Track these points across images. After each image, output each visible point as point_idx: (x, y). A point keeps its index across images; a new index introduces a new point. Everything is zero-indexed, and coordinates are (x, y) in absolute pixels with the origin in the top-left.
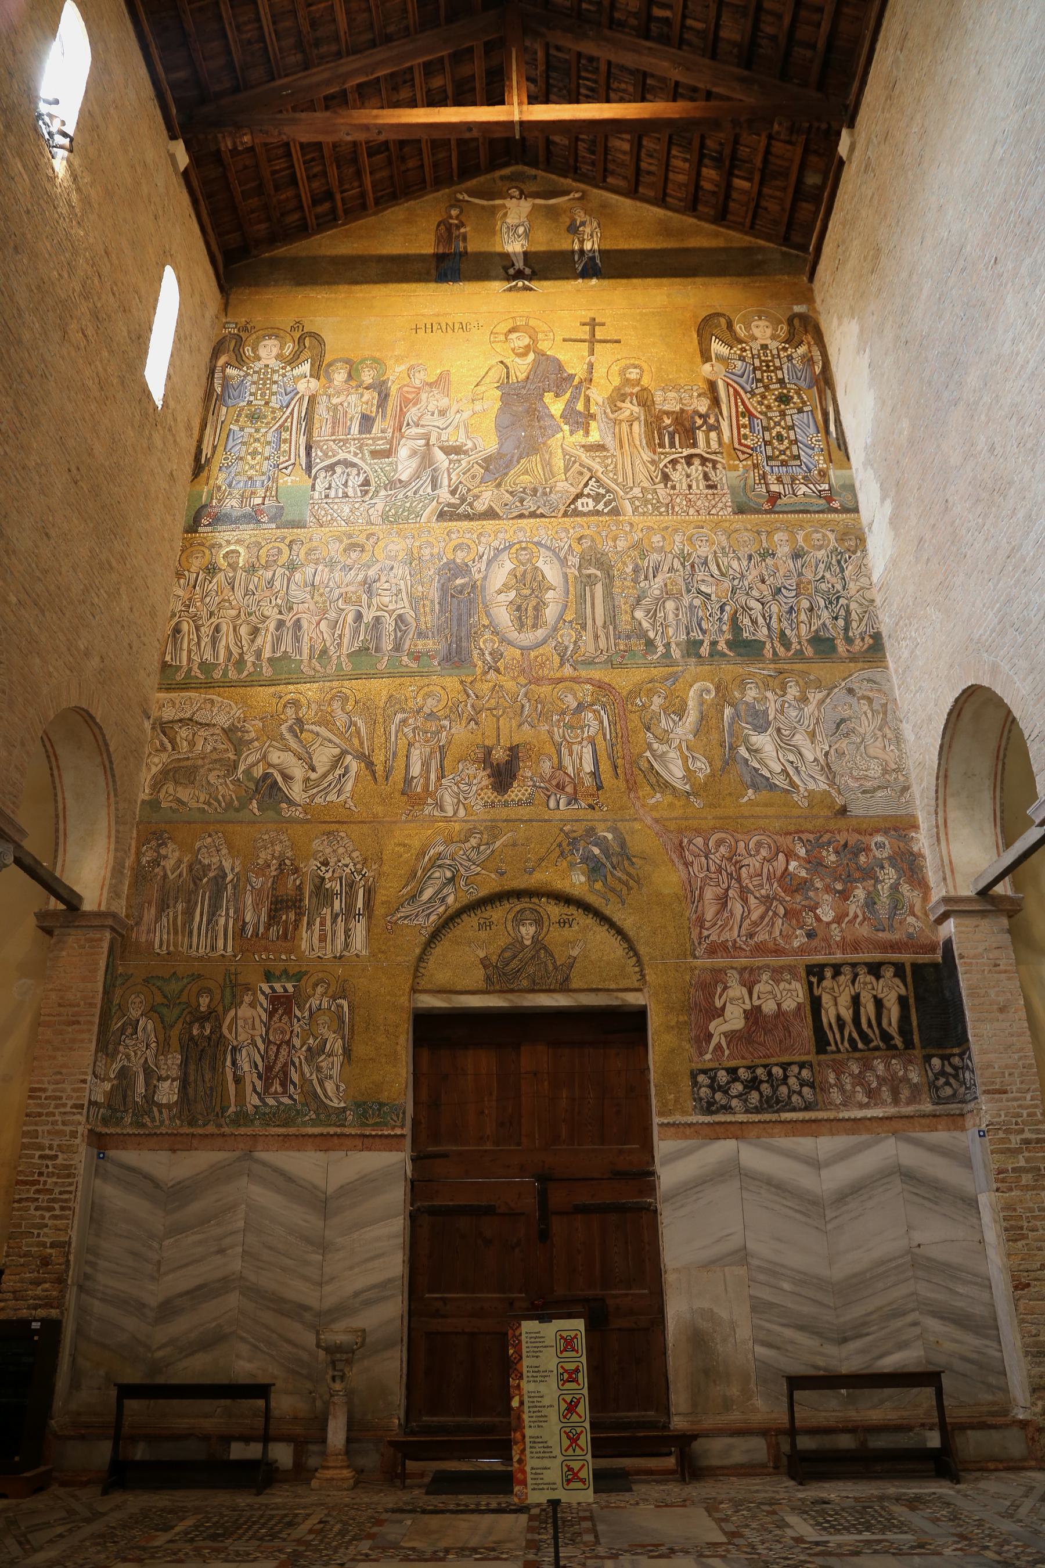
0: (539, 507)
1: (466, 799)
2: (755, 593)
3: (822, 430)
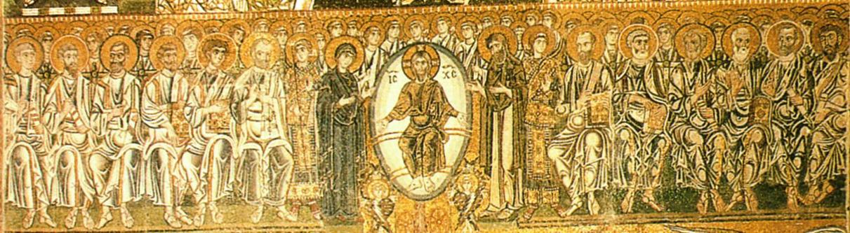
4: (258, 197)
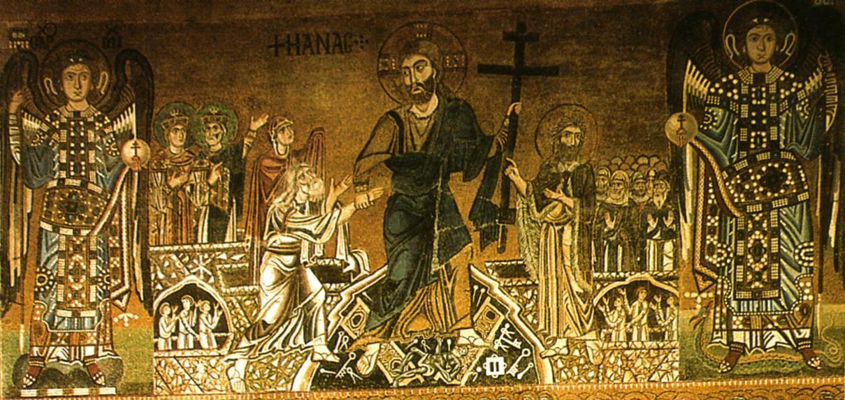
0: (437, 370)
3: (817, 237)
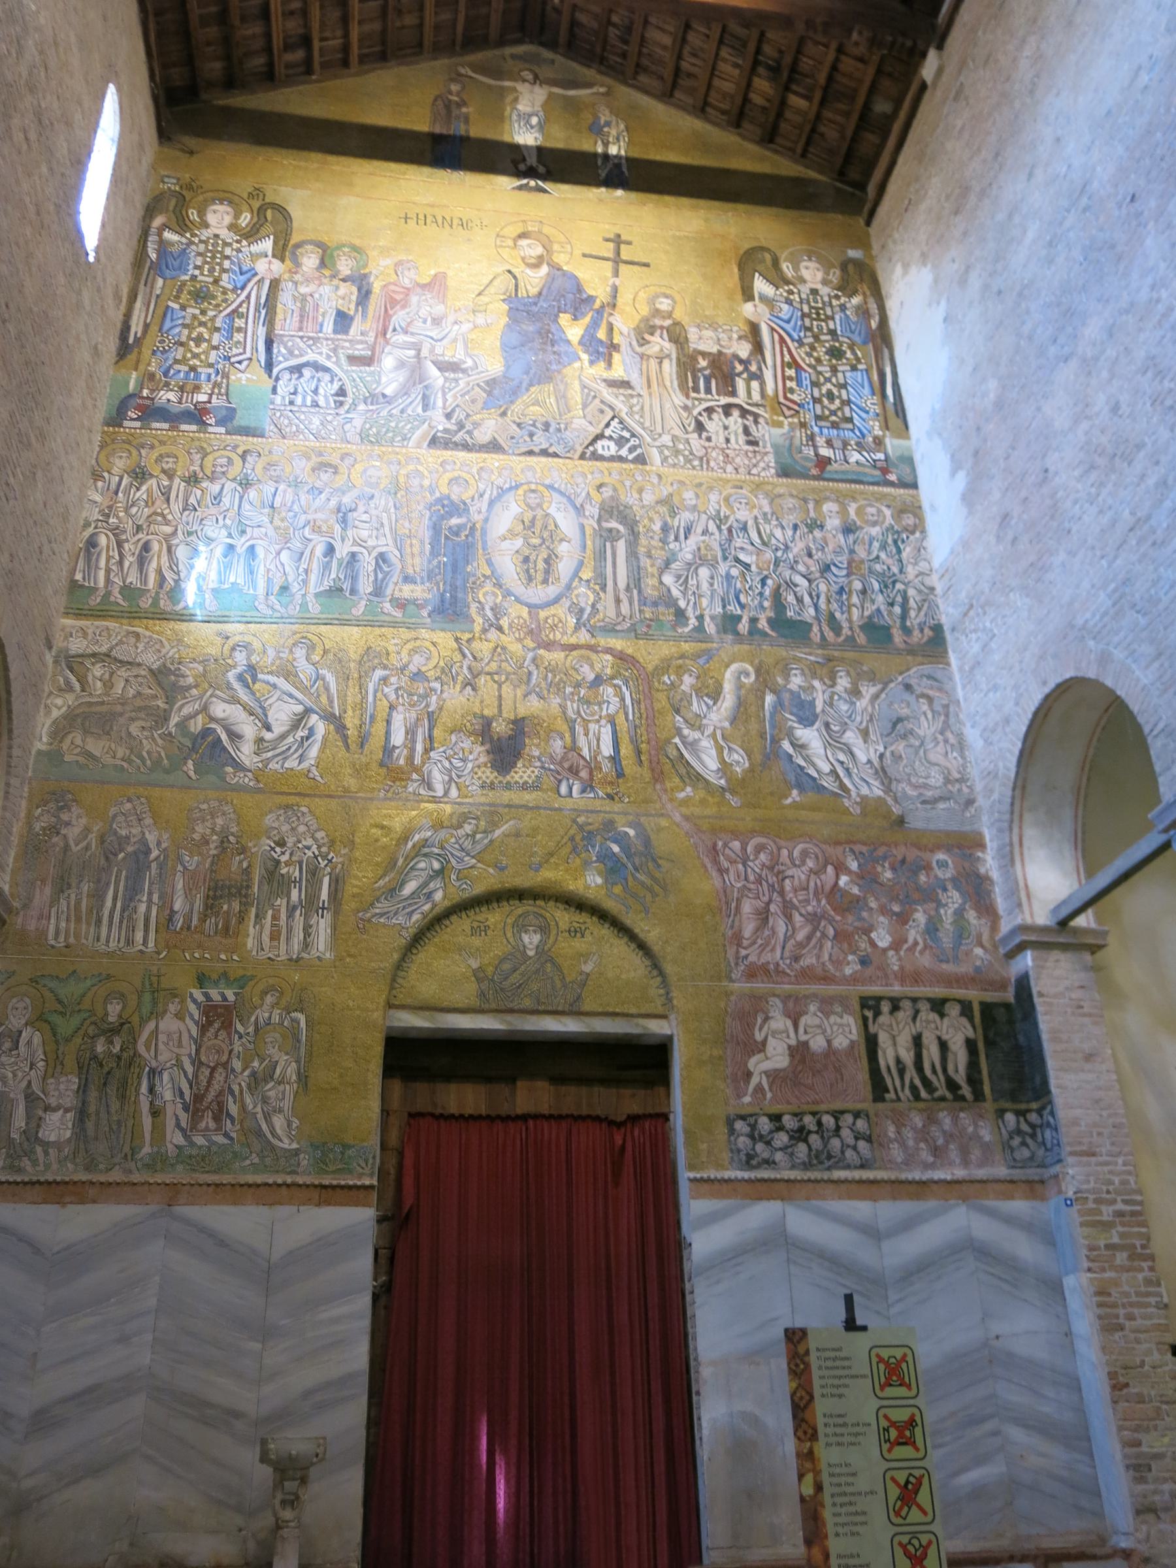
0: (551, 445)
1: (459, 777)
2: (801, 568)
4: (361, 591)
